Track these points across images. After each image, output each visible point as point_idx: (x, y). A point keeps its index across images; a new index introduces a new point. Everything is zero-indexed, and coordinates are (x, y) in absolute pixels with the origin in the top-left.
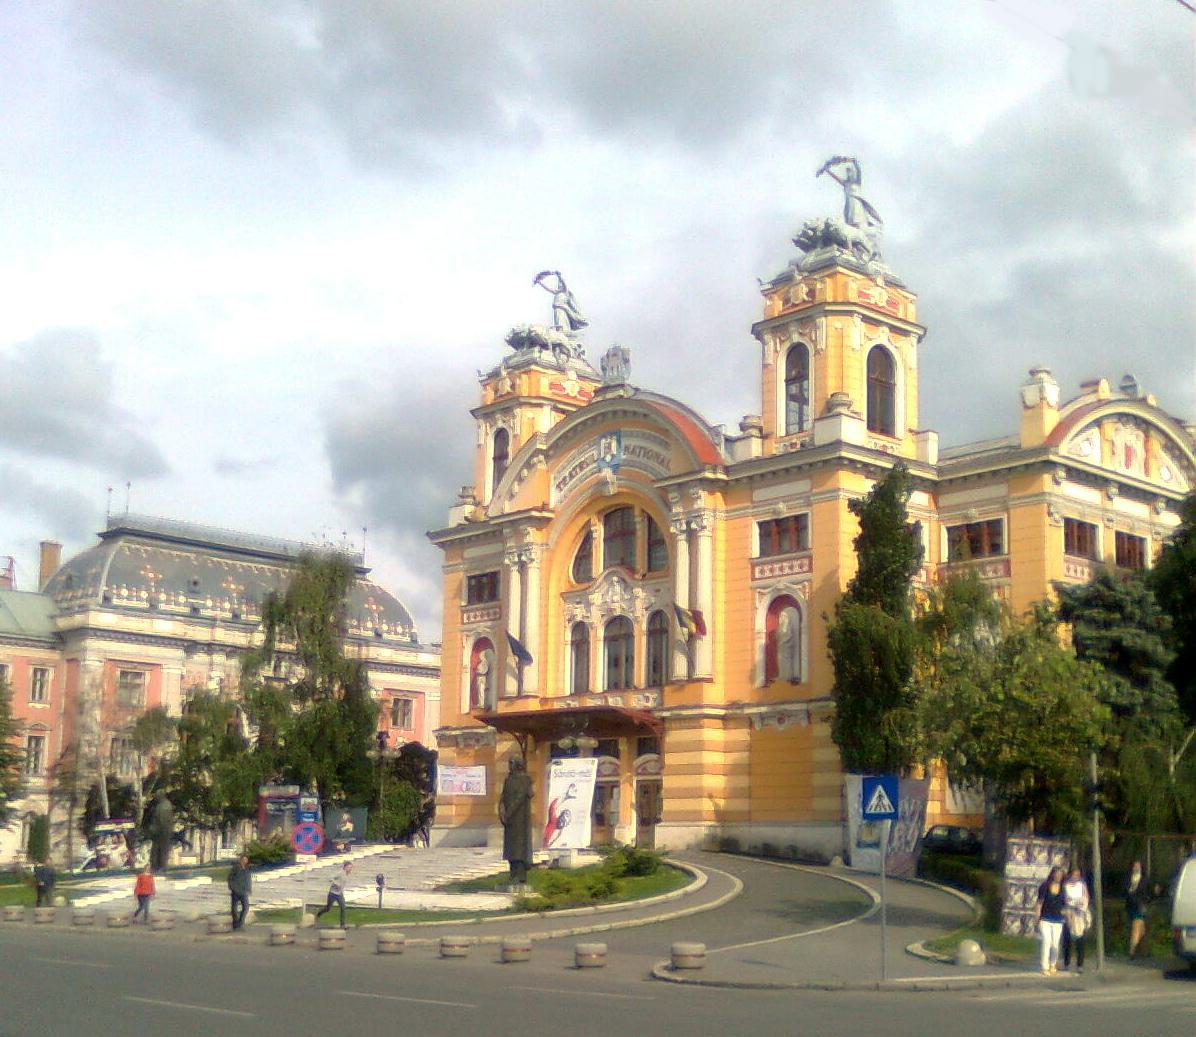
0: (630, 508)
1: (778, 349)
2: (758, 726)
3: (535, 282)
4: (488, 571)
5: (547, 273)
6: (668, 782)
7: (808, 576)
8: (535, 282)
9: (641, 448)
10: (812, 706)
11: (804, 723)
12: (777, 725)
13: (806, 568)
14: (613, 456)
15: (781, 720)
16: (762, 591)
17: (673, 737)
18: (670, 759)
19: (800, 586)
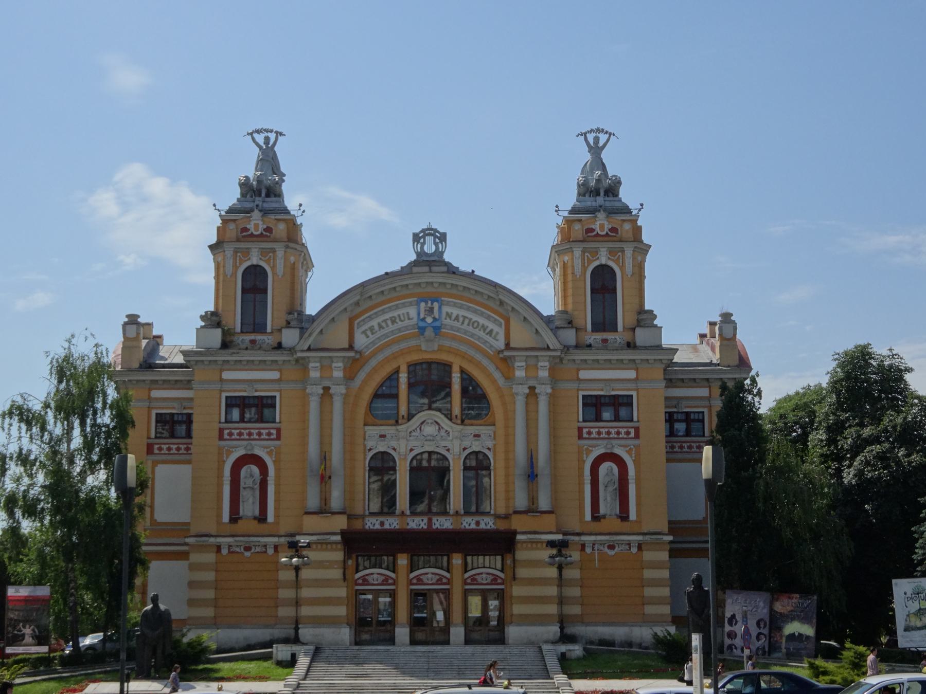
0: (446, 367)
1: (586, 265)
2: (588, 550)
3: (251, 134)
4: (257, 394)
5: (271, 131)
6: (517, 591)
7: (636, 442)
8: (248, 134)
9: (465, 317)
10: (647, 538)
11: (634, 550)
12: (606, 550)
13: (632, 435)
14: (435, 319)
15: (611, 547)
16: (590, 448)
17: (521, 555)
18: (522, 572)
19: (628, 449)
